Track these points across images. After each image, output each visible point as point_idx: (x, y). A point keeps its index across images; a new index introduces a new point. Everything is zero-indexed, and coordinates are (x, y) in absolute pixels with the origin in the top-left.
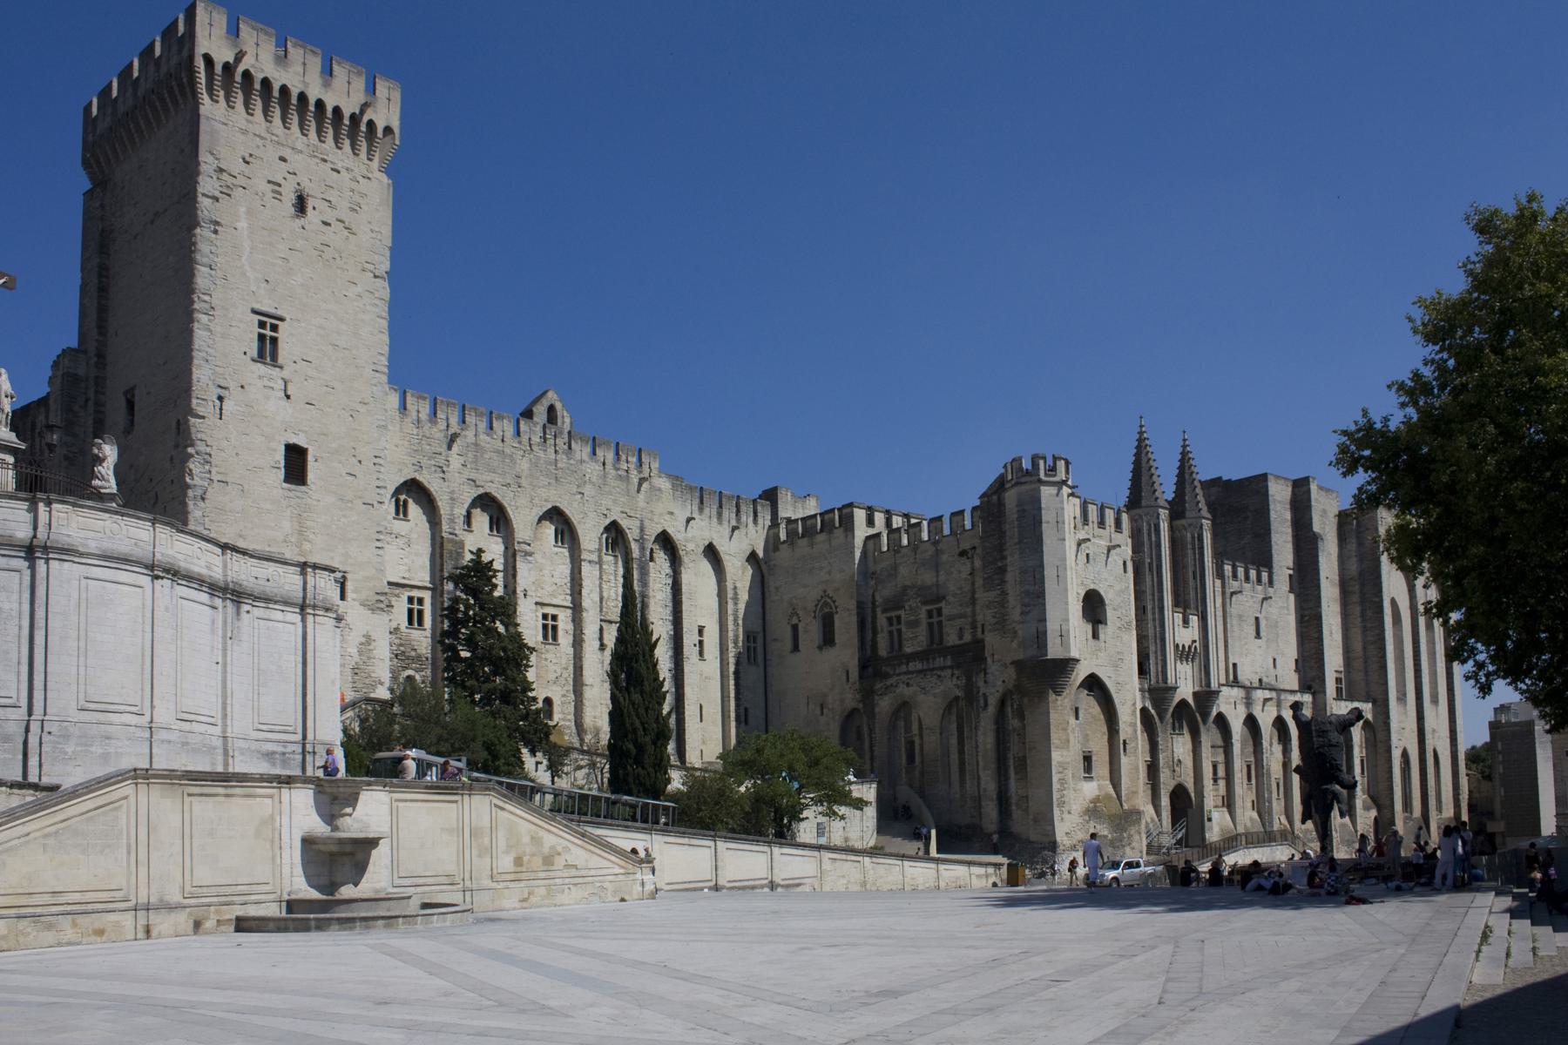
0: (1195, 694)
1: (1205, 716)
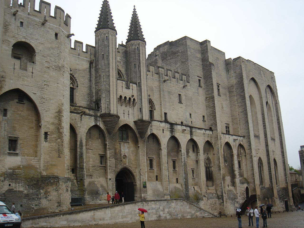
0: (135, 122)
1: (142, 133)
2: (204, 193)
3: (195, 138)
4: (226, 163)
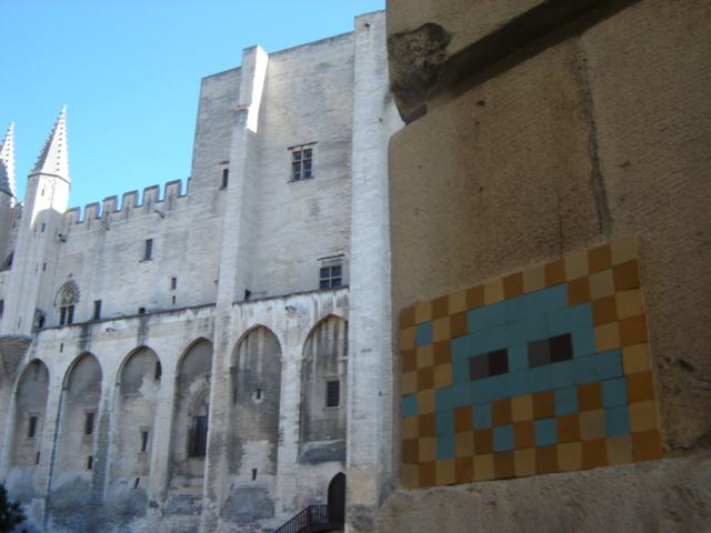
2: (154, 496)
3: (151, 342)
4: (259, 397)
